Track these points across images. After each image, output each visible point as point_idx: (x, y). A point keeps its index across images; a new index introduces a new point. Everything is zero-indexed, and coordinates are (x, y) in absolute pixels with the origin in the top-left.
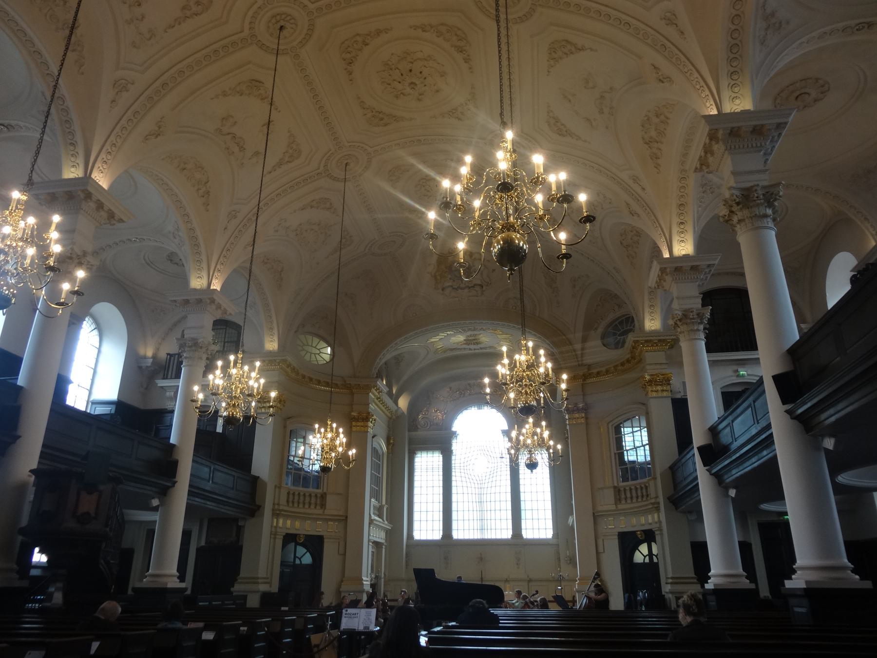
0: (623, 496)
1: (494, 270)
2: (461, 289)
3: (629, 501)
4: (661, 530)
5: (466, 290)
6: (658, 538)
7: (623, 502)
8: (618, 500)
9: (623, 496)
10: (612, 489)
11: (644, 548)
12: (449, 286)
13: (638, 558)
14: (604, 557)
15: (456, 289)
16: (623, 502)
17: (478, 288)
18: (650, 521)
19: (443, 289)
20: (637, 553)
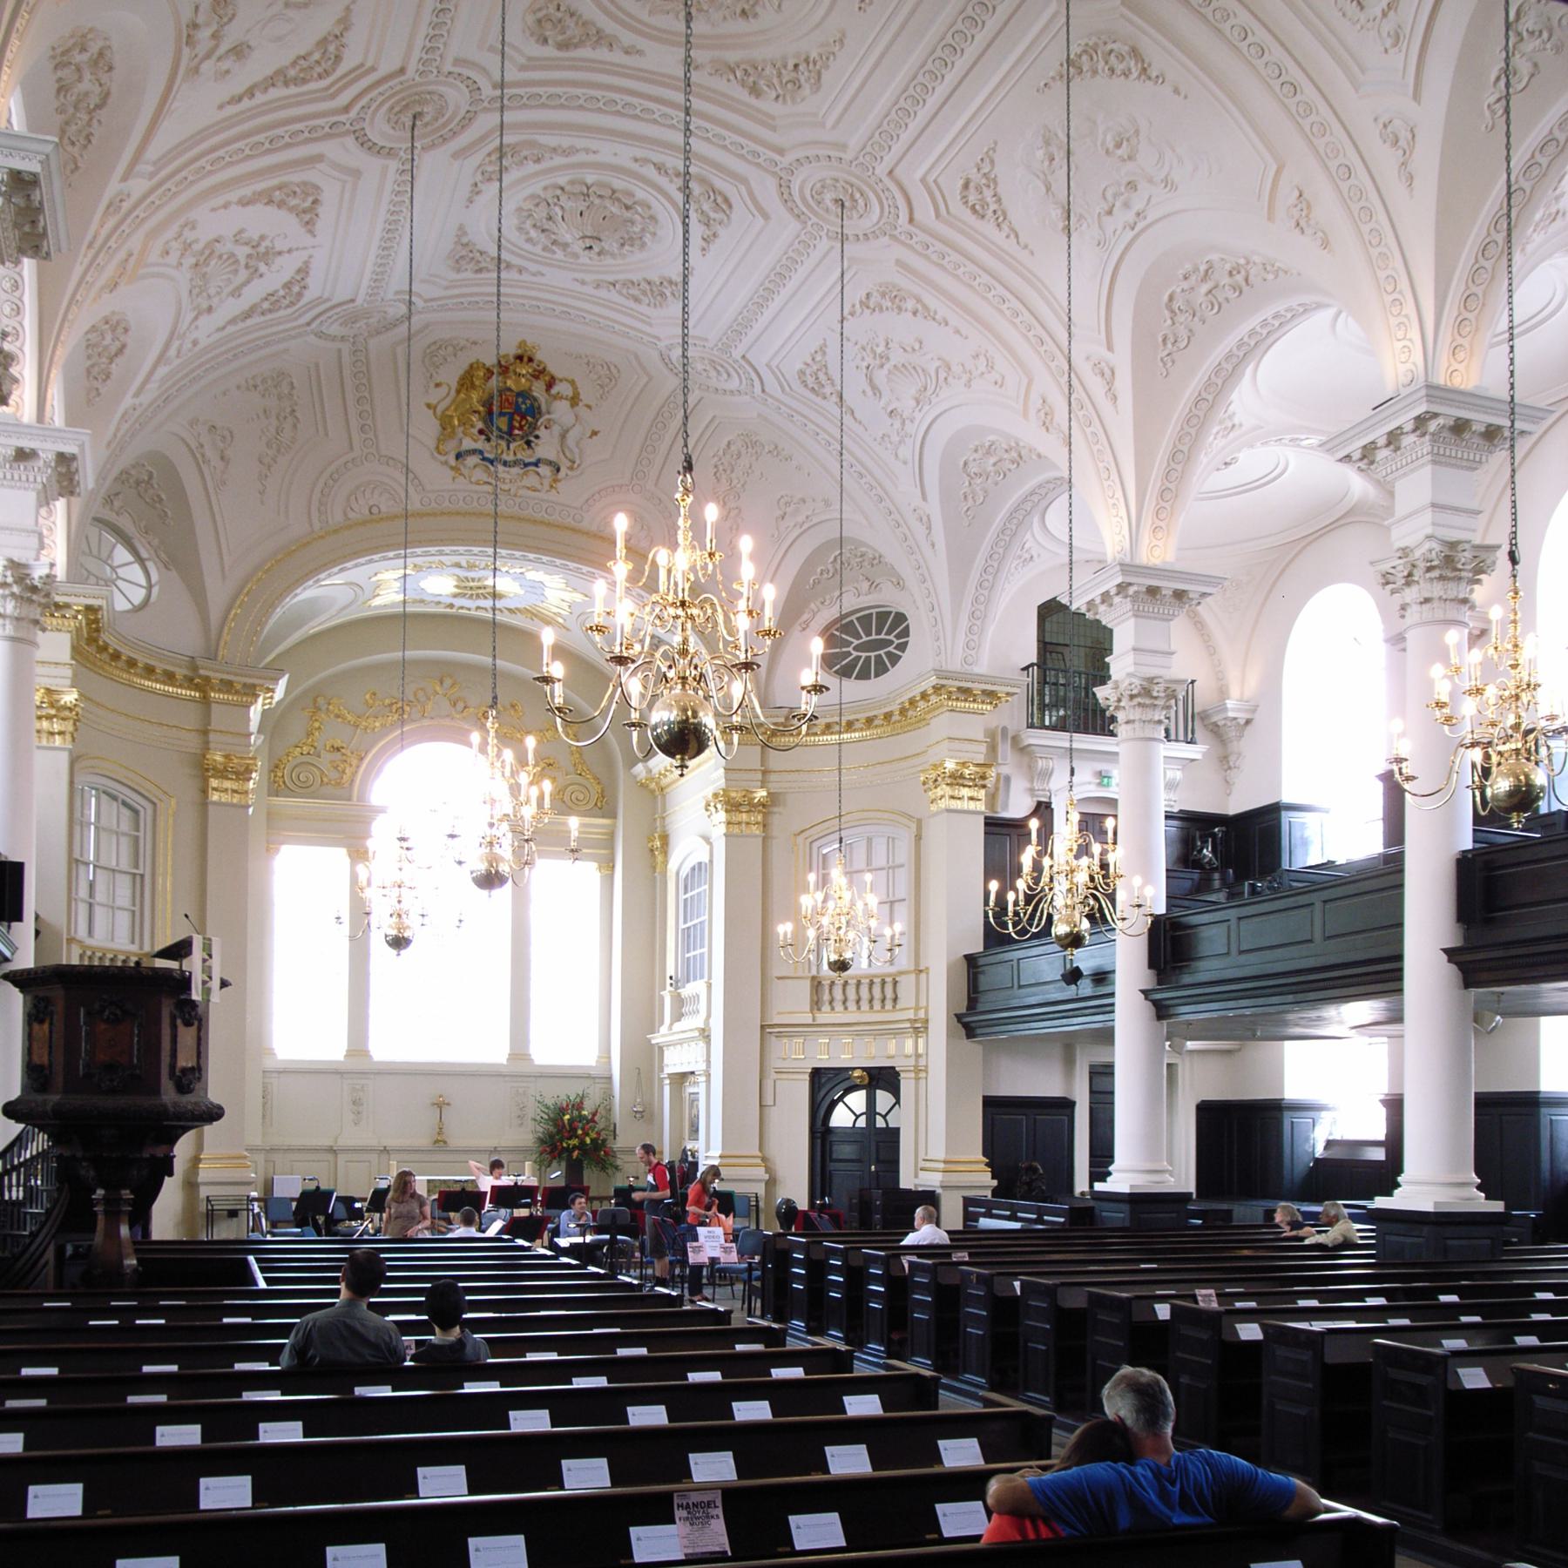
0: (826, 997)
1: (595, 433)
2: (505, 464)
3: (839, 1007)
4: (919, 1071)
5: (516, 470)
6: (906, 1086)
7: (826, 1008)
8: (816, 1004)
9: (826, 997)
10: (808, 982)
11: (857, 1100)
12: (474, 452)
13: (841, 1118)
14: (774, 1114)
15: (492, 462)
16: (826, 1008)
17: (544, 470)
18: (892, 1052)
19: (458, 456)
20: (840, 1107)
